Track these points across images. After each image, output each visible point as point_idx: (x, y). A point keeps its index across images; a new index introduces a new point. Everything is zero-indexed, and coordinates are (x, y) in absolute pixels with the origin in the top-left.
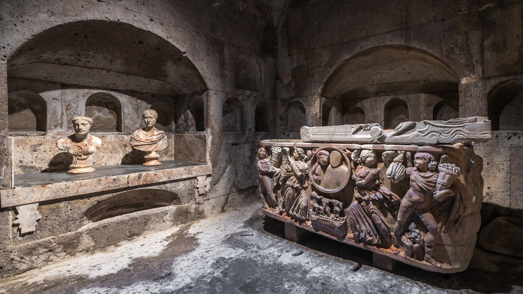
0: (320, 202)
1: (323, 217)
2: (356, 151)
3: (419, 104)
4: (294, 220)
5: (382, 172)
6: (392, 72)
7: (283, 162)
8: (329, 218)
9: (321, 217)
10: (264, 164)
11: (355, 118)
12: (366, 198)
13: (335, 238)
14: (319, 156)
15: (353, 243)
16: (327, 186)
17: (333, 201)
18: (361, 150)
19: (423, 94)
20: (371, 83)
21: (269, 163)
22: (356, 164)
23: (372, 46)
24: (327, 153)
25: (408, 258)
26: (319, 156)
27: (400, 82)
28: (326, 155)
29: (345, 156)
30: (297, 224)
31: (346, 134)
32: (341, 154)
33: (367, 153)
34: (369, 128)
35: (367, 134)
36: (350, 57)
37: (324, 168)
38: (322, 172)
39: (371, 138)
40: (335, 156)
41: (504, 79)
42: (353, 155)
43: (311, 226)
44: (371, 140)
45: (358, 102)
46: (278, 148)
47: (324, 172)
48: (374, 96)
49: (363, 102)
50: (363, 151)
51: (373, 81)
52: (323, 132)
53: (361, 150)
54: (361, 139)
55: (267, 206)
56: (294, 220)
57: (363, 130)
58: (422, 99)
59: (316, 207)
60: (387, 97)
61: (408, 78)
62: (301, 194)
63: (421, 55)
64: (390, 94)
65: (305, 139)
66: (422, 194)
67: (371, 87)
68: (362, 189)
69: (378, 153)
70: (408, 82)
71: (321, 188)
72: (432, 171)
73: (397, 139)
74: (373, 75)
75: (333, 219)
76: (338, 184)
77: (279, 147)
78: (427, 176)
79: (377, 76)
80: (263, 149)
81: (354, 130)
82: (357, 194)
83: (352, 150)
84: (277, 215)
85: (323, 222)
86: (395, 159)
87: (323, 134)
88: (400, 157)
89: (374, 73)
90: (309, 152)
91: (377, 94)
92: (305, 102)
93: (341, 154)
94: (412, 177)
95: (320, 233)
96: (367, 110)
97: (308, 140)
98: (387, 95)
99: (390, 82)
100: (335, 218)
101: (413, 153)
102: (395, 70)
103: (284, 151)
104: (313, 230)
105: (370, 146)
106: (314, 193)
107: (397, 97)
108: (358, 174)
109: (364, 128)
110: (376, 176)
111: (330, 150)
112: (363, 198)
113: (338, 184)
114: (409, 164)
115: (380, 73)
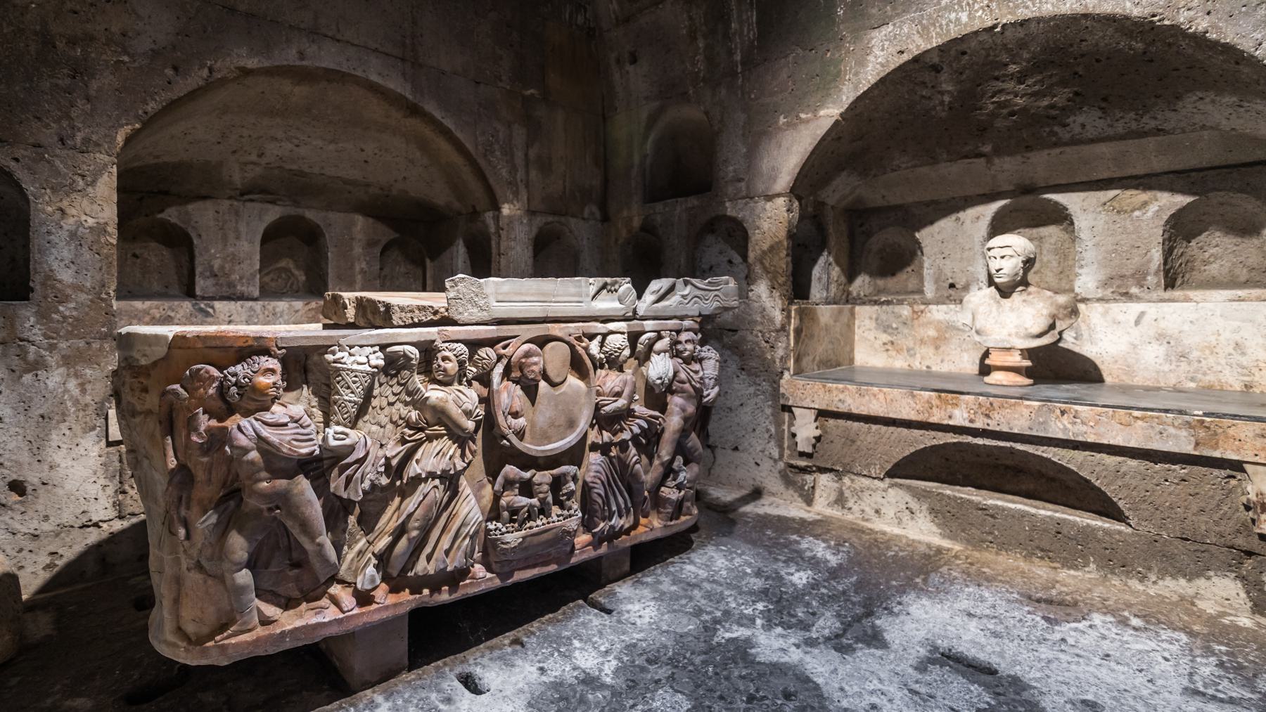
0: (527, 488)
2: (599, 338)
3: (352, 239)
6: (332, 147)
7: (375, 402)
8: (550, 519)
9: (531, 528)
10: (290, 425)
11: (135, 256)
12: (626, 435)
13: (553, 568)
14: (523, 360)
15: (591, 553)
17: (564, 469)
18: (605, 336)
19: (360, 217)
20: (254, 158)
21: (306, 419)
23: (332, 66)
25: (669, 523)
26: (523, 360)
27: (330, 177)
29: (582, 351)
31: (580, 299)
32: (572, 347)
34: (617, 287)
35: (613, 300)
36: (261, 65)
40: (555, 357)
41: (550, 219)
42: (594, 347)
43: (489, 575)
44: (623, 312)
45: (169, 206)
46: (369, 350)
47: (533, 400)
48: (230, 198)
49: (190, 207)
50: (610, 338)
51: (261, 155)
52: (526, 295)
53: (605, 336)
54: (608, 310)
57: (605, 291)
58: (359, 228)
59: (523, 507)
60: (270, 206)
61: (354, 174)
62: (460, 490)
63: (428, 132)
64: (280, 200)
65: (470, 314)
67: (242, 169)
70: (346, 182)
71: (529, 447)
73: (658, 310)
74: (274, 139)
75: (561, 518)
77: (372, 346)
79: (283, 144)
80: (273, 363)
81: (593, 290)
85: (536, 540)
89: (280, 135)
91: (242, 195)
92: (32, 172)
93: (572, 347)
95: (521, 576)
96: (204, 236)
97: (485, 316)
98: (273, 202)
99: (307, 170)
100: (565, 512)
102: (341, 145)
105: (622, 326)
106: (510, 470)
107: (300, 211)
108: (607, 388)
109: (609, 287)
111: (542, 342)
112: (616, 440)
115: (297, 139)
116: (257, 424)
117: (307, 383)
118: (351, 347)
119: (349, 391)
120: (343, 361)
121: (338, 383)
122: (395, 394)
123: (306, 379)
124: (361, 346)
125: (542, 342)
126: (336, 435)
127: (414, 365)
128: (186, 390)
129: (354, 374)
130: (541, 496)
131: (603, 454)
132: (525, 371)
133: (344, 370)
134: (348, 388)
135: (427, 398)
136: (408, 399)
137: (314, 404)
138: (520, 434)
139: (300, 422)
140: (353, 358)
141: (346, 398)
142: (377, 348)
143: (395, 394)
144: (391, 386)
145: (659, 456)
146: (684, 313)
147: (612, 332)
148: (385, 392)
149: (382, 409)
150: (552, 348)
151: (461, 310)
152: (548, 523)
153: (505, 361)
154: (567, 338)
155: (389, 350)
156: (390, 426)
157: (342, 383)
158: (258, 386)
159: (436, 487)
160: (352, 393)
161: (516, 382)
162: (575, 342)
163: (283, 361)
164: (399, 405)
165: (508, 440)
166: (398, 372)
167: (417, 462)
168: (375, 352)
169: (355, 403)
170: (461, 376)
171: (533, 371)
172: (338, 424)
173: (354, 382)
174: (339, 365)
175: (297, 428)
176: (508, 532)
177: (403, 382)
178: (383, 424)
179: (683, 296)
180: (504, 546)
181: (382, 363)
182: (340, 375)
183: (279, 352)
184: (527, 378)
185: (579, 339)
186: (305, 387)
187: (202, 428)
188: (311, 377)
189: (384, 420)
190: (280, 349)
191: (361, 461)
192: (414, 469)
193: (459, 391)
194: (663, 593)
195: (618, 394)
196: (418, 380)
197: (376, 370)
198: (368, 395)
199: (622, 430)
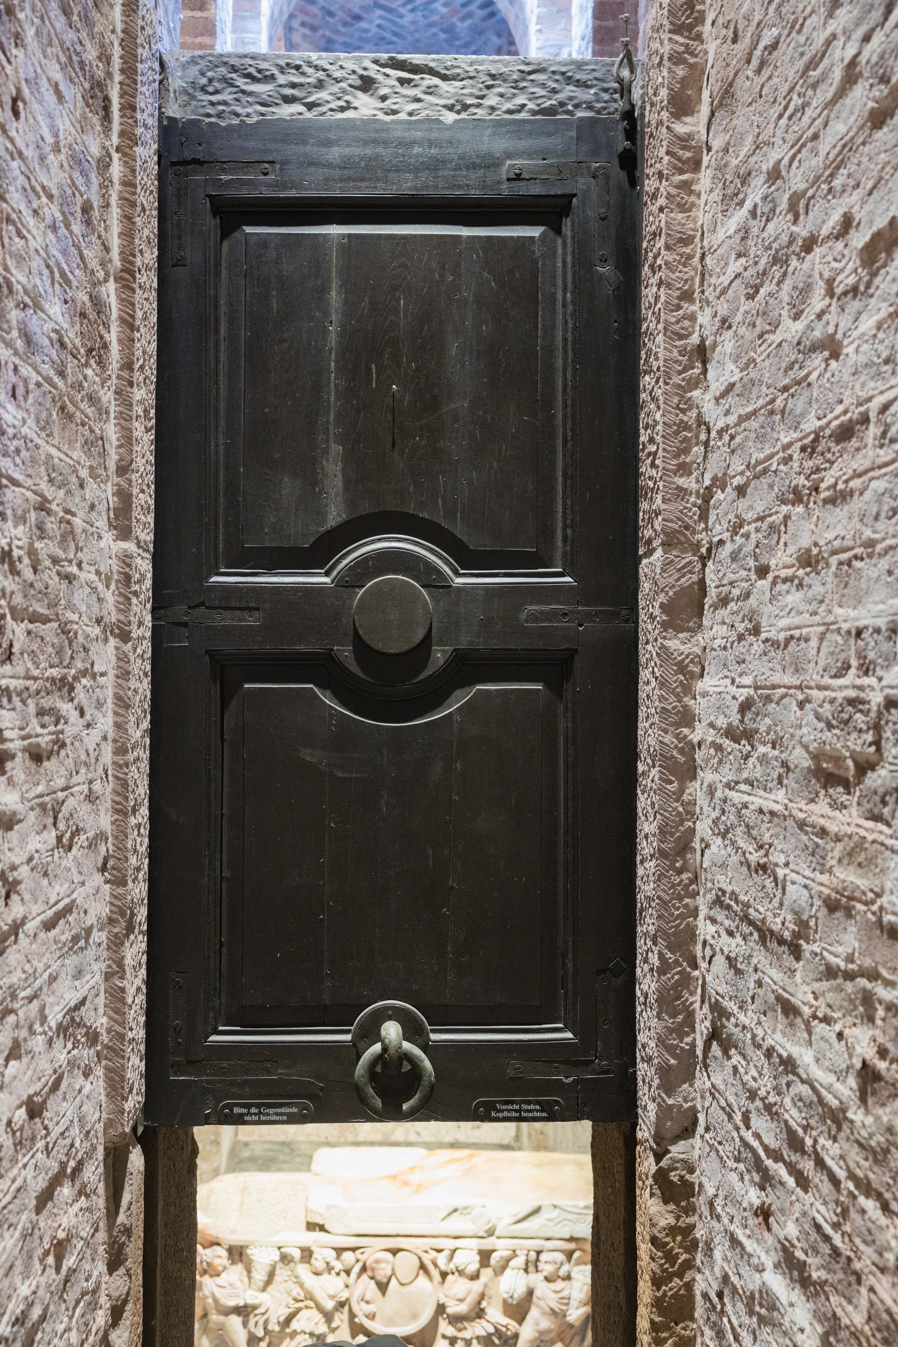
5: (490, 1285)
12: (467, 1334)
16: (391, 1322)
21: (239, 1284)
22: (444, 1275)
24: (389, 1256)
28: (388, 1262)
32: (420, 1258)
33: (468, 1259)
37: (383, 1287)
38: (378, 1293)
40: (405, 1264)
57: (456, 1214)
66: (553, 1318)
68: (456, 1320)
69: (485, 1256)
72: (564, 1279)
76: (414, 1316)
78: (558, 1289)
80: (224, 1253)
82: (445, 1328)
83: (439, 1251)
86: (512, 1263)
88: (520, 1261)
90: (348, 1257)
93: (420, 1258)
94: (537, 1293)
101: (539, 1253)
103: (285, 1259)
108: (451, 1293)
110: (482, 1296)
111: (395, 1252)
112: (460, 1335)
113: (414, 1316)
114: (531, 1269)
125: (395, 1252)
126: (251, 1297)
138: (372, 1317)
146: (549, 1235)
148: (282, 1273)
161: (372, 1278)
170: (329, 1269)
179: (549, 1220)
188: (244, 1259)
192: (295, 1325)
195: (461, 1300)
196: (303, 1270)
198: (271, 1275)
199: (465, 1328)
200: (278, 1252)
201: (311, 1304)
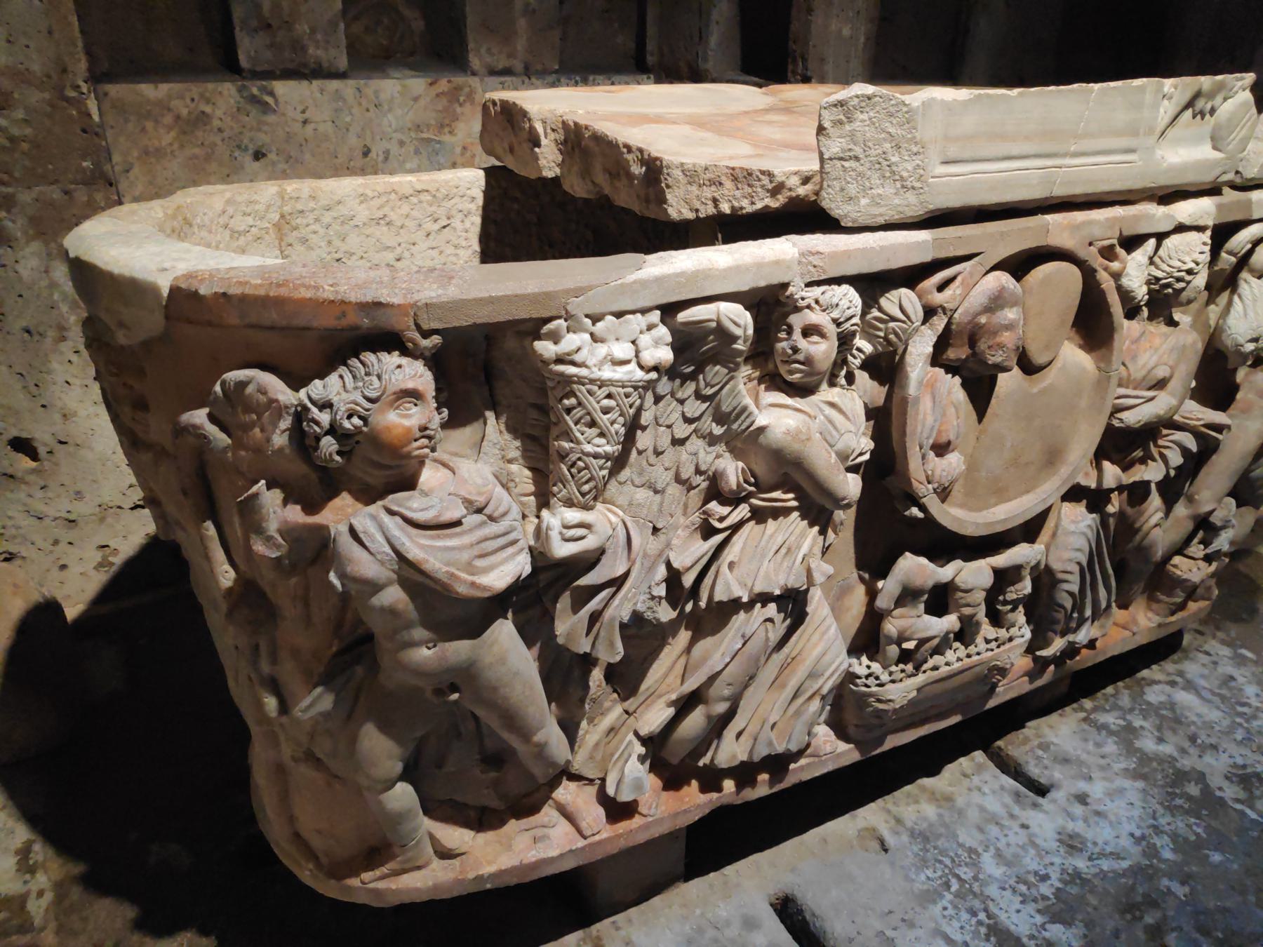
1: (947, 664)
4: (729, 785)
8: (972, 649)
9: (935, 668)
29: (1107, 283)
30: (762, 788)
39: (1216, 163)
46: (638, 321)
54: (1185, 167)
55: (454, 836)
56: (729, 785)
75: (994, 645)
77: (644, 311)
80: (417, 375)
81: (1166, 110)
84: (604, 835)
87: (1015, 151)
95: (894, 741)
97: (913, 206)
104: (855, 756)
111: (1020, 265)
116: (392, 524)
117: (494, 407)
118: (596, 319)
119: (595, 431)
120: (578, 358)
121: (569, 411)
122: (688, 421)
123: (492, 395)
124: (619, 315)
125: (1020, 265)
127: (740, 353)
128: (224, 429)
129: (605, 391)
130: (967, 611)
131: (1091, 509)
132: (982, 345)
133: (581, 381)
134: (593, 424)
135: (762, 430)
136: (718, 430)
137: (514, 453)
138: (944, 493)
139: (487, 511)
140: (602, 350)
141: (588, 448)
142: (655, 316)
143: (688, 421)
144: (682, 402)
145: (1191, 500)
147: (1181, 228)
149: (658, 453)
150: (1047, 280)
151: (852, 189)
152: (969, 656)
153: (940, 323)
154: (1083, 253)
155: (683, 316)
156: (674, 490)
157: (578, 413)
158: (386, 437)
159: (770, 620)
160: (602, 435)
162: (1097, 262)
163: (435, 362)
164: (696, 444)
165: (923, 508)
166: (700, 369)
167: (731, 565)
168: (650, 327)
169: (607, 457)
171: (1001, 346)
172: (569, 503)
173: (606, 411)
174: (571, 370)
175: (482, 524)
176: (893, 681)
177: (709, 391)
178: (659, 486)
180: (881, 706)
181: (665, 355)
182: (572, 394)
183: (426, 343)
184: (984, 363)
185: (1108, 253)
186: (490, 415)
187: (272, 527)
189: (663, 477)
190: (426, 334)
191: (617, 583)
193: (832, 405)
194: (1145, 758)
197: (654, 375)
200: (663, 332)
201: (789, 499)
